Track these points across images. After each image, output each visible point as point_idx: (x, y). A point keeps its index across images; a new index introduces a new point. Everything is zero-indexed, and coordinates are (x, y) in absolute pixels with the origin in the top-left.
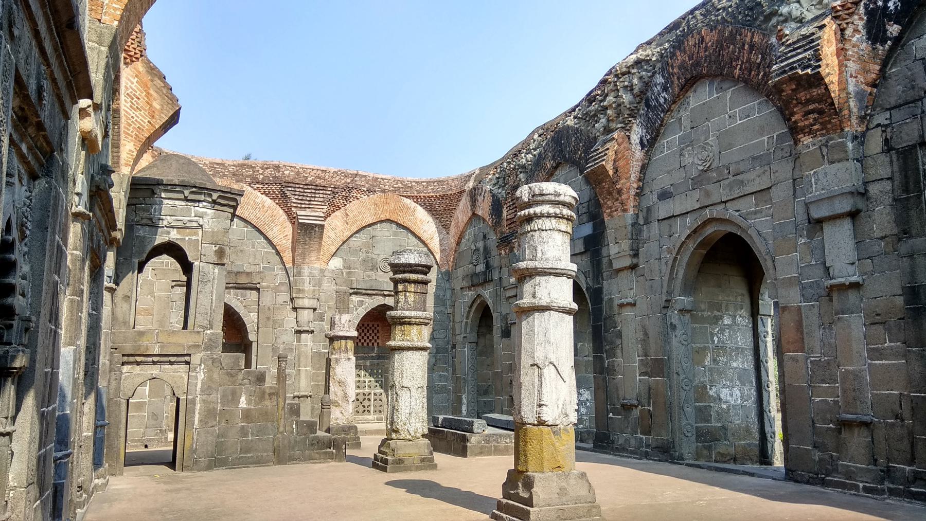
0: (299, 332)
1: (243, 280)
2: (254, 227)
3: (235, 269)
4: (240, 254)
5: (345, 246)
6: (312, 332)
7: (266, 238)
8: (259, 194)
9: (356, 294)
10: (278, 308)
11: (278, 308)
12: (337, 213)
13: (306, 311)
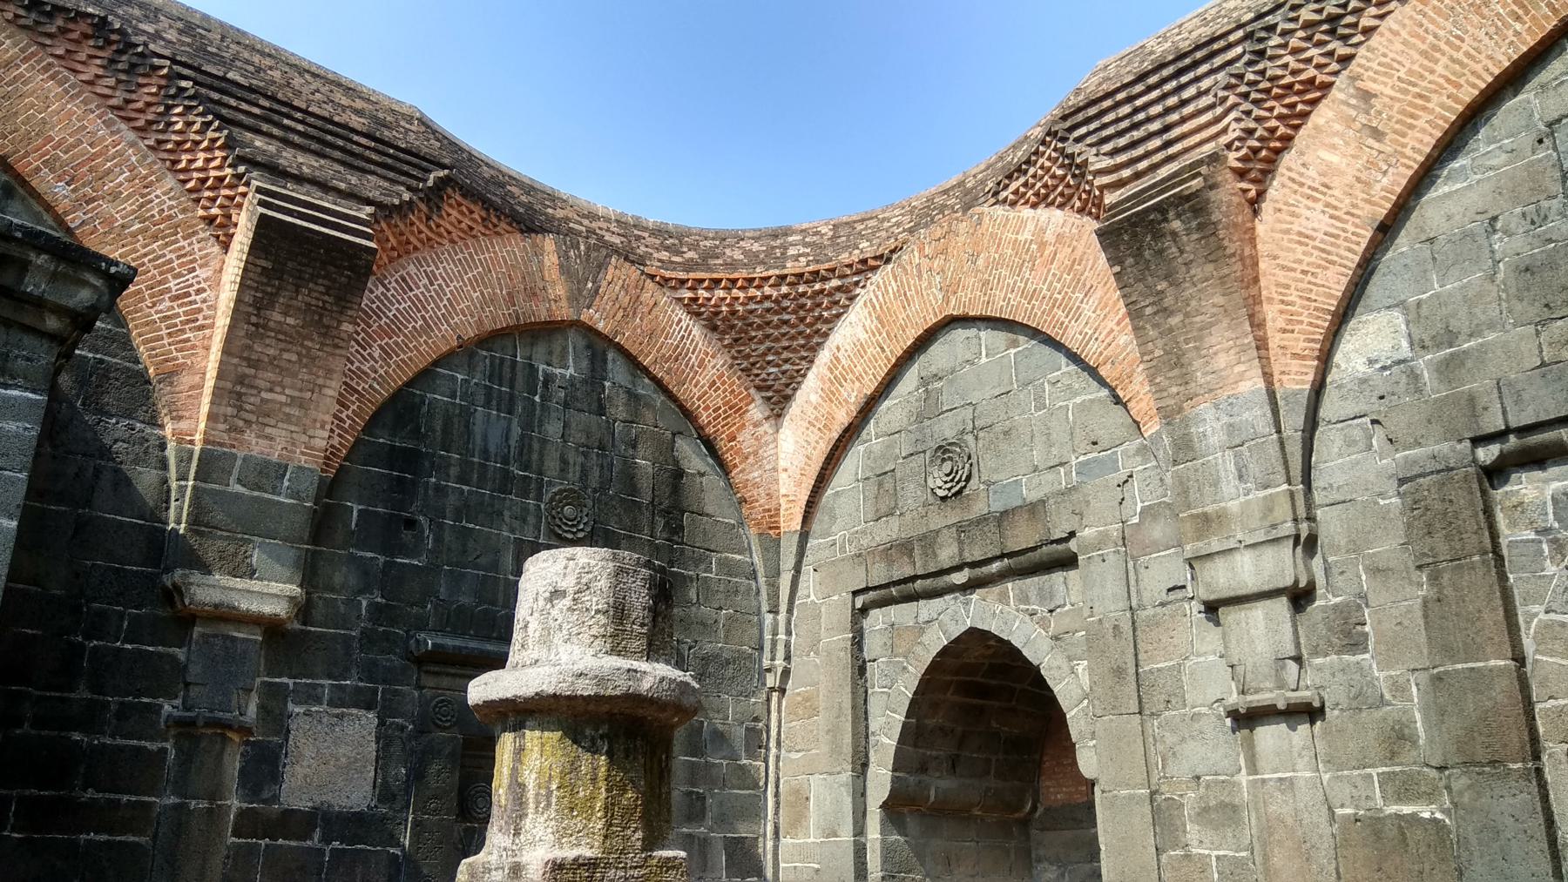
0: (1247, 719)
1: (1022, 536)
2: (1035, 333)
3: (997, 506)
4: (1003, 446)
5: (1404, 243)
6: (1310, 713)
7: (1074, 358)
8: (1027, 212)
9: (1536, 459)
10: (1154, 623)
11: (1154, 623)
12: (1323, 115)
13: (1258, 611)
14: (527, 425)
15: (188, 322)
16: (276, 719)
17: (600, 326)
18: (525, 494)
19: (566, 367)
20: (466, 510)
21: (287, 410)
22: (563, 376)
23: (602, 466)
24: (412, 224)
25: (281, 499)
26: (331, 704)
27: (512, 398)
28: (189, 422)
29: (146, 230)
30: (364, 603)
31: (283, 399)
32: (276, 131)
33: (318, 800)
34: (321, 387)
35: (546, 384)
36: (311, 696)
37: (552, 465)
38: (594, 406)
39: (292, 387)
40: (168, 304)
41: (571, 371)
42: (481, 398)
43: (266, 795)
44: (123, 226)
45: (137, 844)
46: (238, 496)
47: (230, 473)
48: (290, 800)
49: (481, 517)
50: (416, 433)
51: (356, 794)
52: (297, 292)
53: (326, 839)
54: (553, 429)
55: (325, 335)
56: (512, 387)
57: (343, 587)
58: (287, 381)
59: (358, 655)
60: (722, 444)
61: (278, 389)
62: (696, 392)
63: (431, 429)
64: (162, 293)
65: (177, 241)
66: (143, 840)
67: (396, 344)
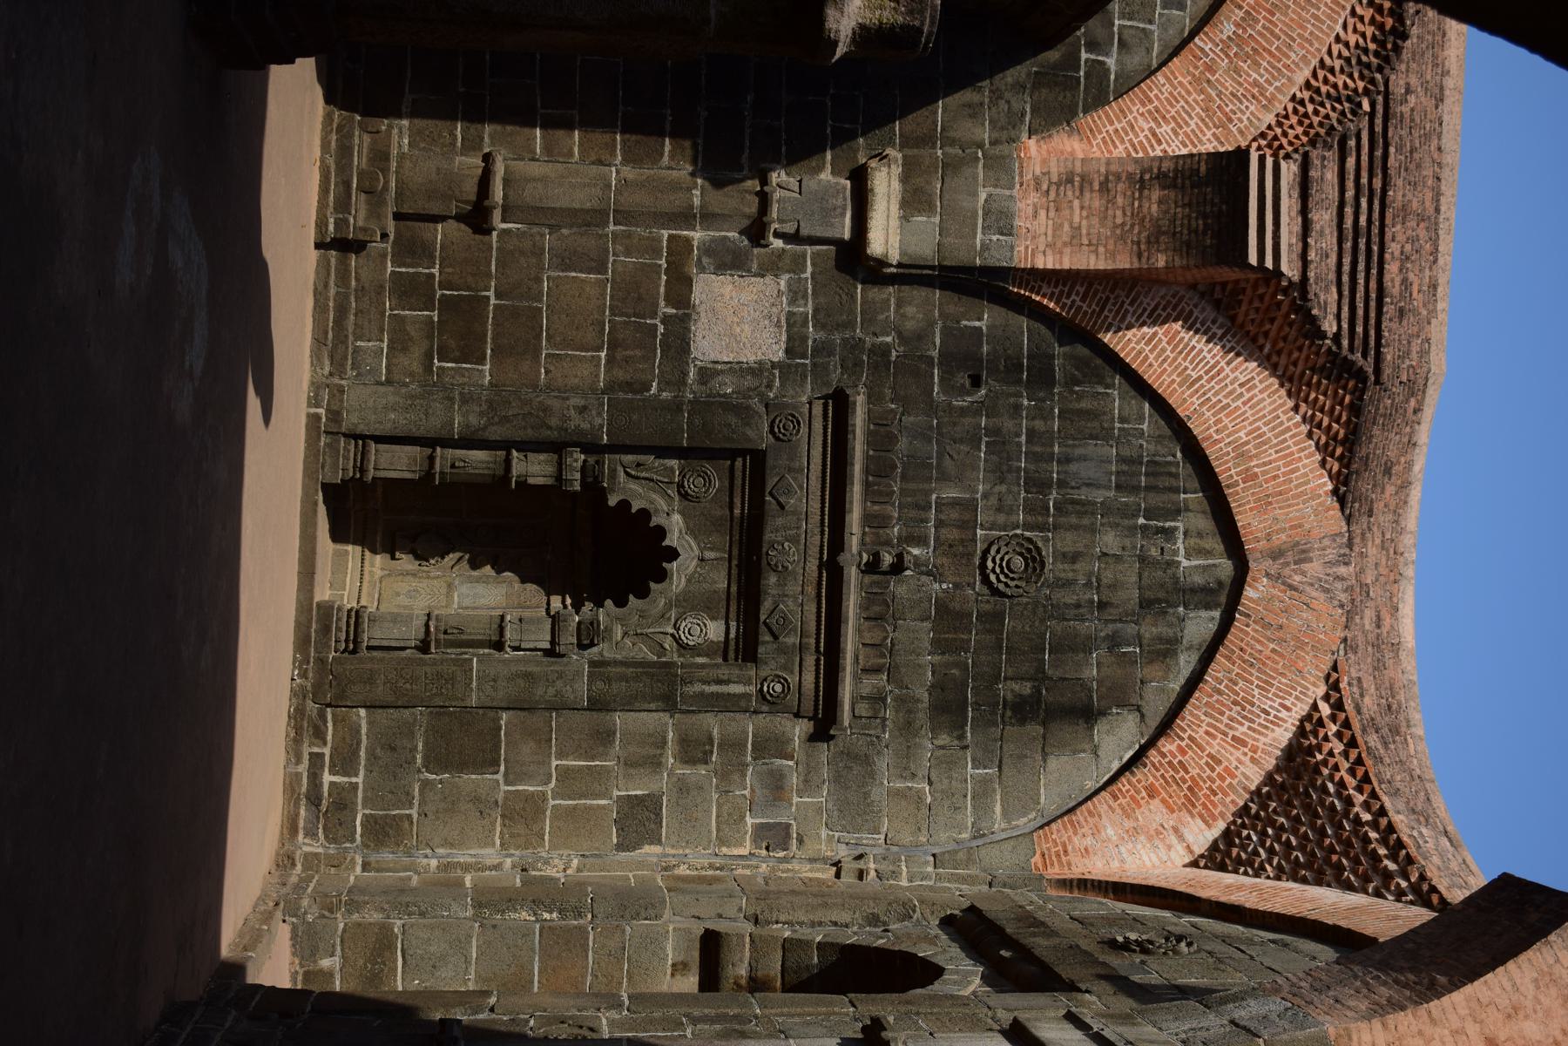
14: (1107, 508)
15: (1133, 145)
16: (771, 267)
17: (1249, 592)
18: (1029, 509)
19: (1188, 556)
20: (1000, 444)
21: (1066, 227)
22: (1176, 553)
23: (1078, 606)
24: (1300, 349)
25: (979, 236)
26: (790, 314)
27: (1135, 489)
28: (1040, 154)
29: (1211, 100)
30: (889, 339)
31: (1077, 219)
32: (1350, 194)
33: (701, 309)
34: (1096, 252)
35: (1163, 531)
36: (796, 294)
37: (1069, 541)
38: (1149, 594)
39: (1089, 227)
40: (1146, 126)
41: (1185, 563)
42: (1126, 452)
43: (705, 260)
44: (1208, 81)
45: (662, 155)
46: (975, 195)
47: (996, 186)
48: (701, 284)
49: (994, 458)
50: (1072, 381)
51: (708, 345)
52: (1184, 206)
53: (666, 320)
54: (1110, 540)
55: (1149, 242)
56: (1148, 488)
57: (904, 316)
58: (1095, 221)
59: (837, 338)
60: (1142, 775)
61: (1085, 213)
62: (1200, 734)
63: (1080, 396)
64: (1155, 120)
65: (1209, 128)
66: (666, 158)
67: (1163, 350)
